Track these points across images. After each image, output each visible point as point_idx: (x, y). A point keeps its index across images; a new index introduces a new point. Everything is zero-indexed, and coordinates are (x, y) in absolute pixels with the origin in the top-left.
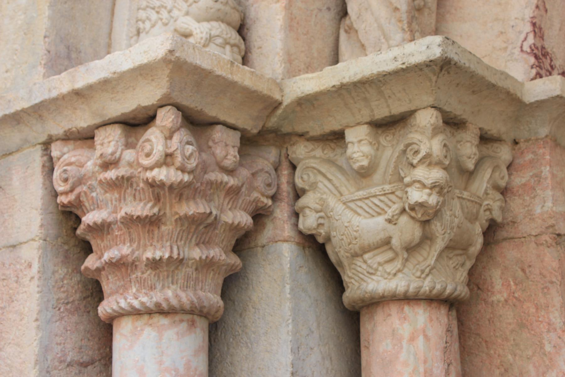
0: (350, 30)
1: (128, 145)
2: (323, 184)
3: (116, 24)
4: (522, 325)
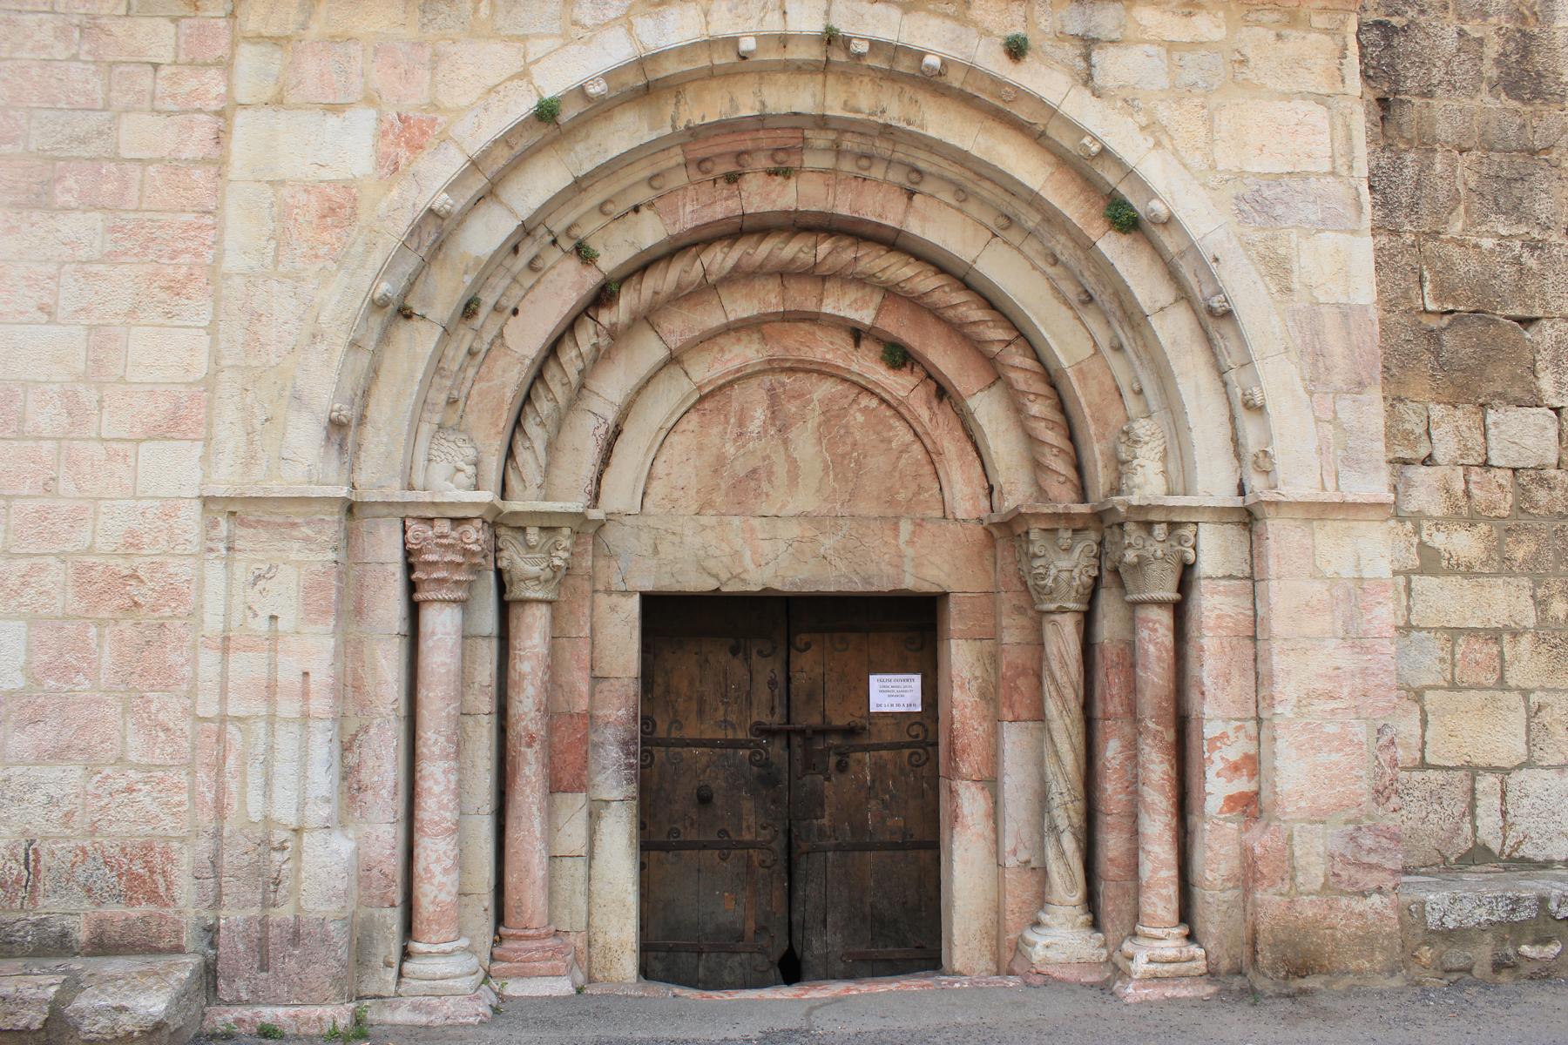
0: (516, 469)
1: (453, 530)
2: (511, 548)
3: (416, 452)
4: (571, 612)
